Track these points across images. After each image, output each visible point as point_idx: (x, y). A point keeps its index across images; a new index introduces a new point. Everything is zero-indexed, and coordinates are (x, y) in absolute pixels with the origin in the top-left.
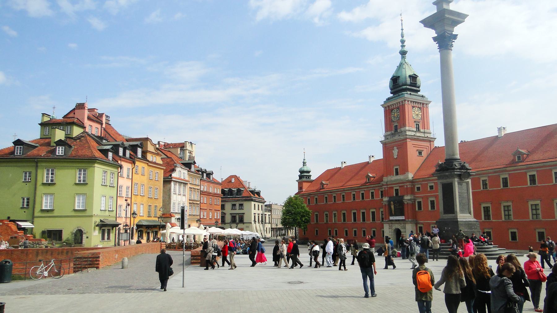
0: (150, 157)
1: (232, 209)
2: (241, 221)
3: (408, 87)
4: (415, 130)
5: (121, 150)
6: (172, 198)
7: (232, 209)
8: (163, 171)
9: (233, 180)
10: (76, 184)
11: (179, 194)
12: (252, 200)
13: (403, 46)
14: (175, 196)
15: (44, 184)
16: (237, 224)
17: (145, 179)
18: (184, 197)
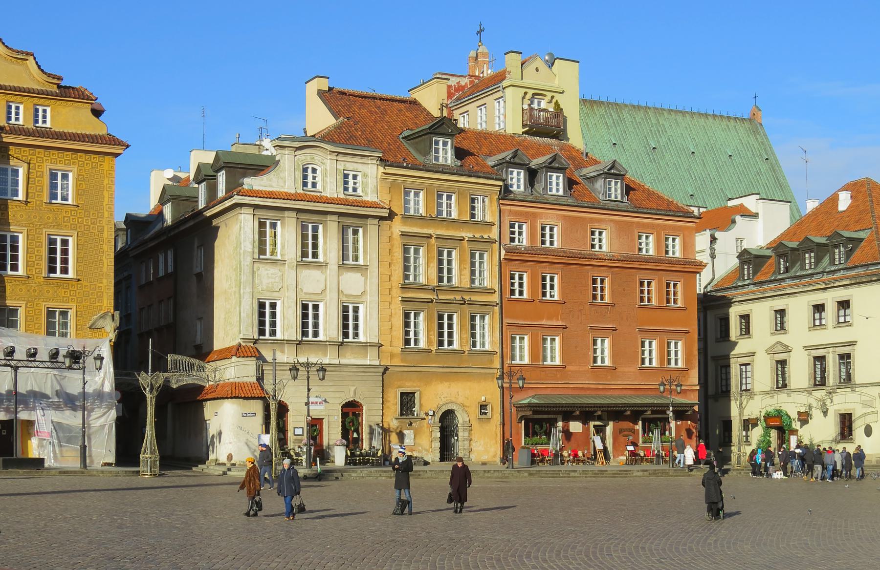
2: (848, 380)
14: (267, 275)
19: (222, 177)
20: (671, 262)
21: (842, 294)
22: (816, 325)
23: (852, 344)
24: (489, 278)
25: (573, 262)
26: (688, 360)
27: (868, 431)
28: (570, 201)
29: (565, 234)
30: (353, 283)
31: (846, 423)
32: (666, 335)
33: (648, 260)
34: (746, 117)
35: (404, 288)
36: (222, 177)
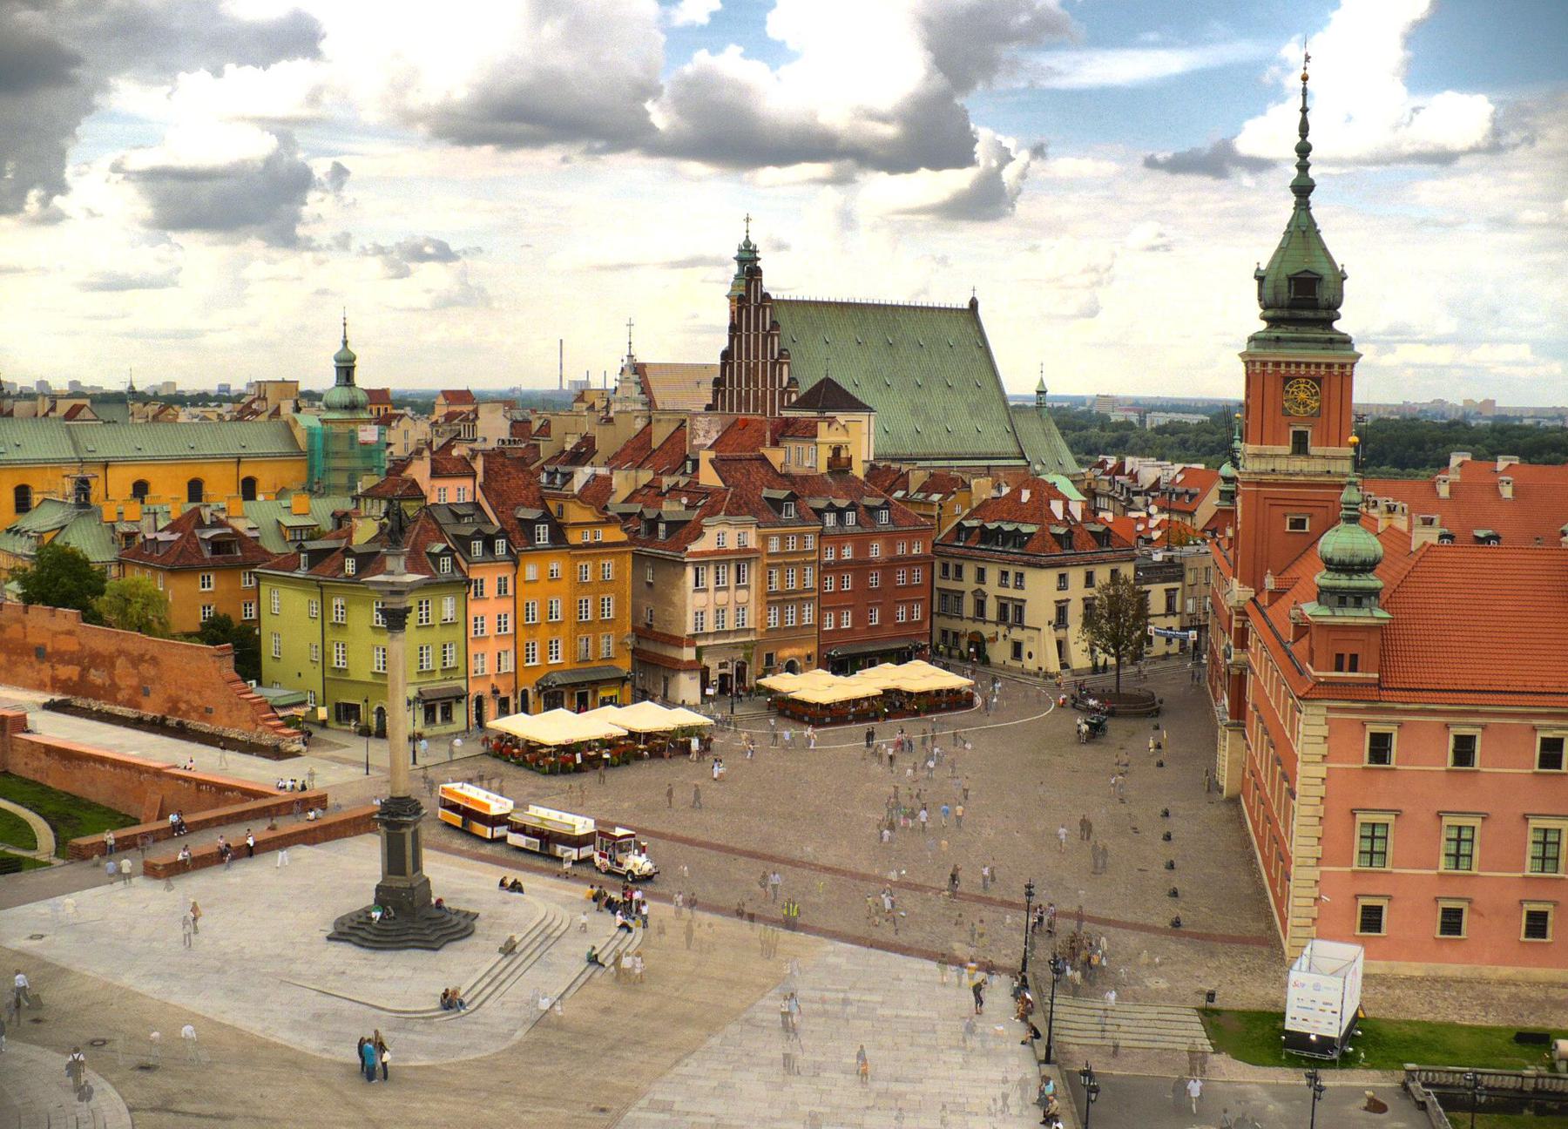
0: (574, 537)
1: (1001, 585)
2: (1019, 622)
3: (1279, 313)
4: (1288, 449)
5: (477, 546)
6: (689, 601)
7: (1001, 585)
8: (629, 557)
9: (1026, 496)
10: (373, 628)
11: (717, 589)
12: (1042, 567)
13: (1303, 167)
14: (701, 599)
15: (333, 624)
16: (1010, 627)
17: (564, 586)
18: (743, 592)
19: (662, 527)
20: (916, 558)
21: (1020, 569)
22: (1003, 584)
23: (1024, 601)
24: (811, 581)
25: (861, 567)
26: (924, 615)
27: (1030, 655)
28: (859, 529)
29: (855, 553)
30: (742, 595)
31: (1017, 649)
32: (909, 603)
33: (900, 559)
34: (966, 306)
35: (768, 594)
36: (662, 527)
